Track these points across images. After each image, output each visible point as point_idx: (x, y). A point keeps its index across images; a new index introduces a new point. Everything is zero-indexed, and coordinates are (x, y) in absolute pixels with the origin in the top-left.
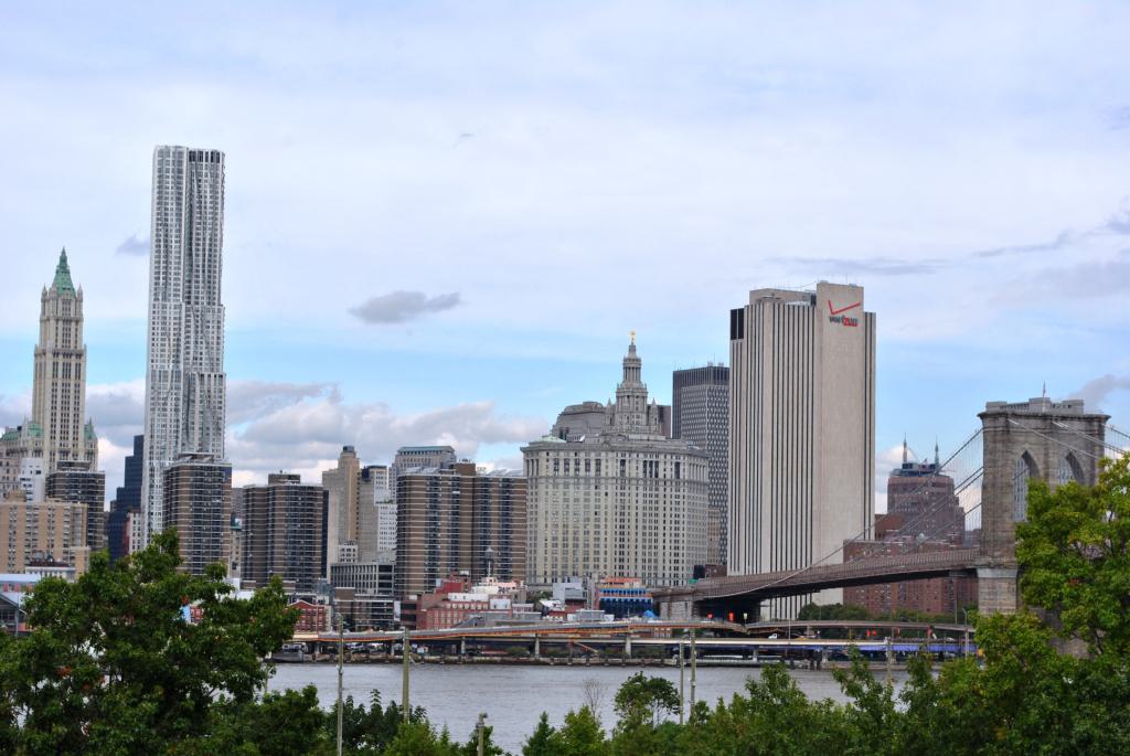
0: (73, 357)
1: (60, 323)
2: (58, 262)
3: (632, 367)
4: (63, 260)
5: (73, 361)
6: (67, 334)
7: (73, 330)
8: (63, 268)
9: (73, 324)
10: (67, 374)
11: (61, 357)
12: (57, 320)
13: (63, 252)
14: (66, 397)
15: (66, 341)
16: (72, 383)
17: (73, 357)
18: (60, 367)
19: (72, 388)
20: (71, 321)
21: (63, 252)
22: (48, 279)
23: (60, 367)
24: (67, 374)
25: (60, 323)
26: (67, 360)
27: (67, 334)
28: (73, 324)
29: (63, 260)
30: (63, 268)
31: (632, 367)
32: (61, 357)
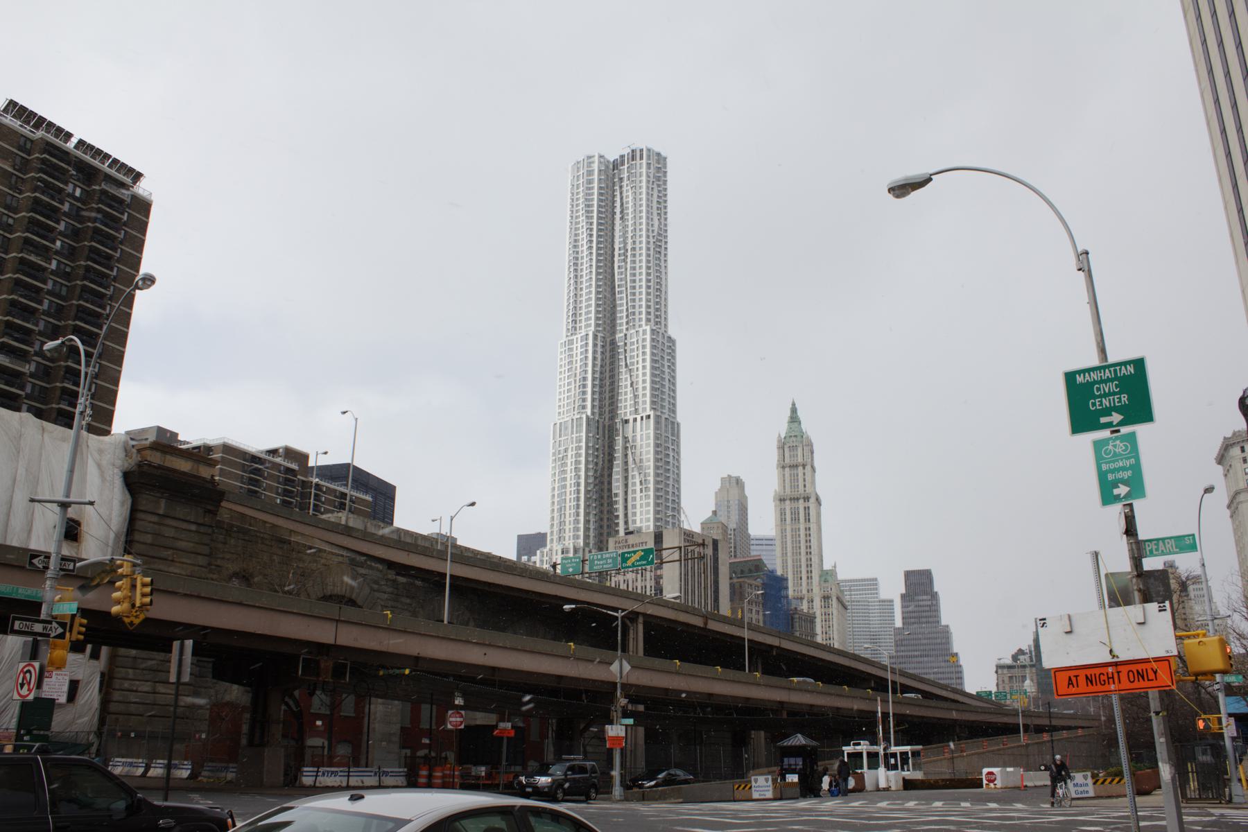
0: (801, 501)
1: (787, 470)
2: (789, 414)
4: (794, 410)
5: (801, 504)
6: (794, 479)
7: (801, 475)
8: (794, 418)
9: (800, 468)
10: (795, 519)
11: (788, 502)
12: (783, 467)
13: (794, 404)
14: (796, 541)
15: (794, 486)
16: (802, 527)
17: (801, 501)
18: (788, 512)
19: (802, 532)
20: (797, 466)
21: (794, 404)
22: (782, 428)
23: (788, 512)
24: (795, 519)
25: (787, 470)
26: (795, 505)
27: (794, 479)
28: (800, 468)
29: (794, 410)
30: (794, 418)
32: (788, 502)
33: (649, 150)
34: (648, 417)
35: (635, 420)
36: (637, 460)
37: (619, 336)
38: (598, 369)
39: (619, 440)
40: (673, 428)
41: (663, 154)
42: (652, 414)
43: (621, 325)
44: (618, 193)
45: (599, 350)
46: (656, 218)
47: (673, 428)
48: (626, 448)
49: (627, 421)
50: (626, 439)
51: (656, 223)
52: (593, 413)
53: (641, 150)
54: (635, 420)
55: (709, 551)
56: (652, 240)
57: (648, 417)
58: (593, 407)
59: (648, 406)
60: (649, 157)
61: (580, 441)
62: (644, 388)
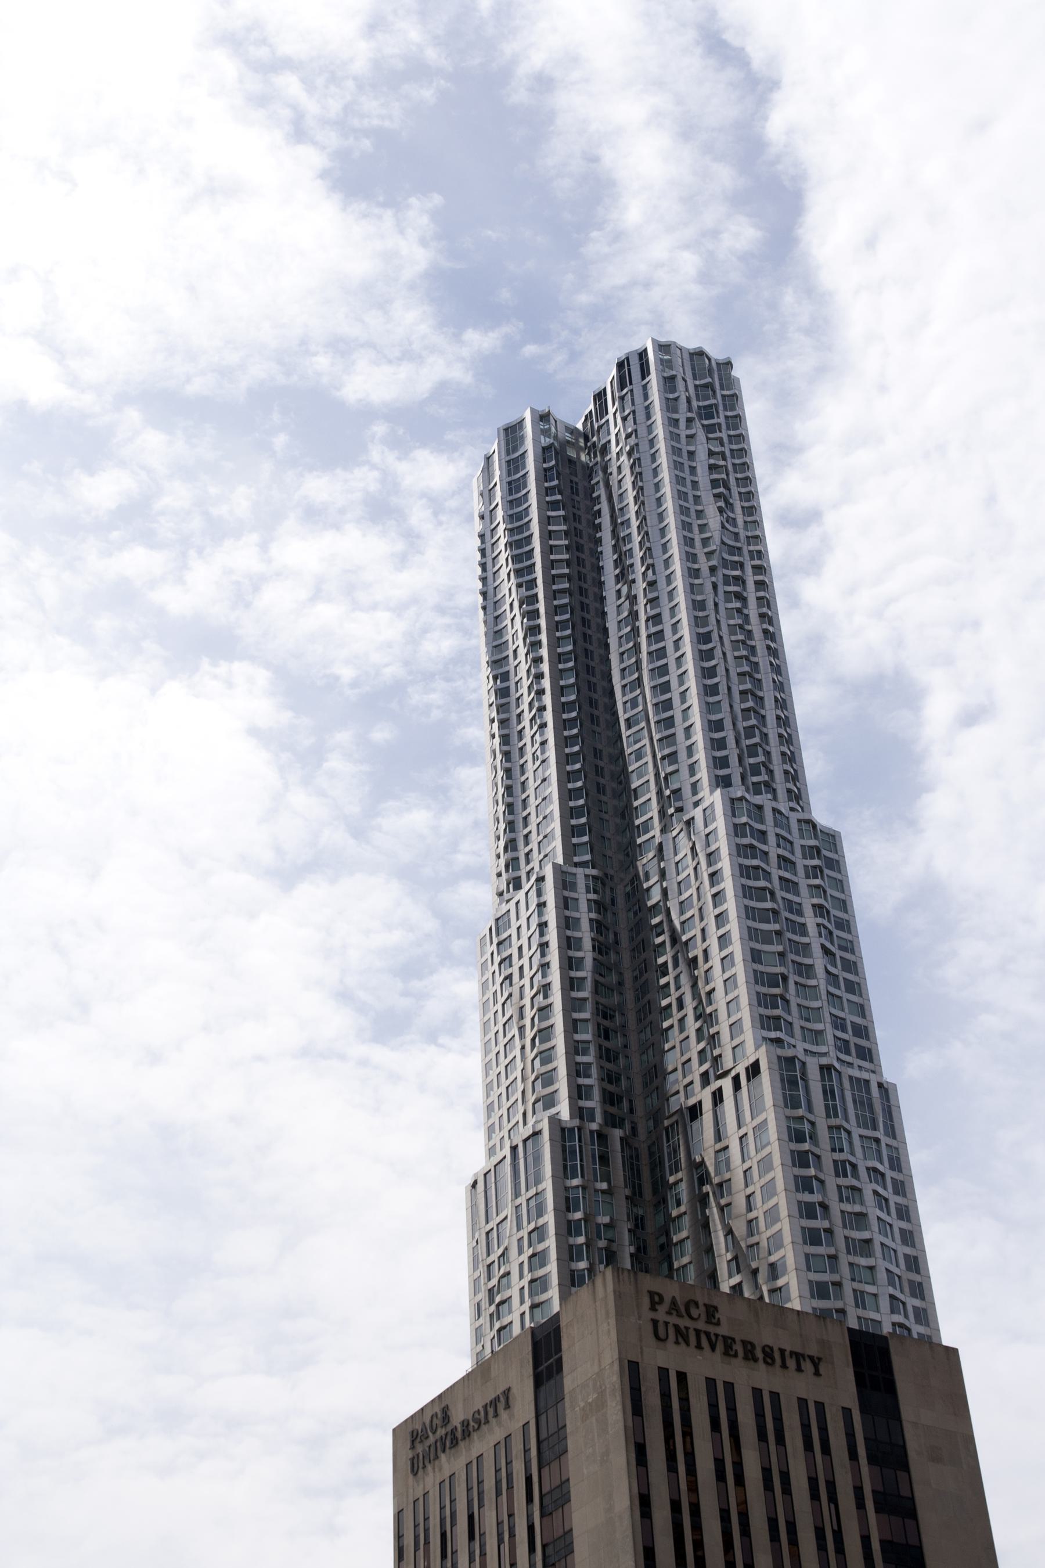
3: (817, 1373)
31: (817, 1373)
33: (664, 348)
34: (754, 1070)
35: (718, 1097)
36: (740, 1228)
37: (647, 860)
38: (586, 972)
39: (680, 1180)
40: (864, 1104)
41: (716, 353)
42: (762, 1055)
43: (646, 827)
44: (601, 492)
45: (584, 915)
46: (711, 510)
47: (864, 1104)
48: (704, 1200)
49: (695, 1111)
50: (699, 1173)
51: (714, 520)
52: (578, 1112)
53: (643, 355)
54: (718, 1097)
55: (840, 1389)
56: (703, 565)
57: (754, 1070)
58: (578, 1093)
59: (748, 1035)
60: (665, 364)
61: (540, 1212)
62: (730, 982)
